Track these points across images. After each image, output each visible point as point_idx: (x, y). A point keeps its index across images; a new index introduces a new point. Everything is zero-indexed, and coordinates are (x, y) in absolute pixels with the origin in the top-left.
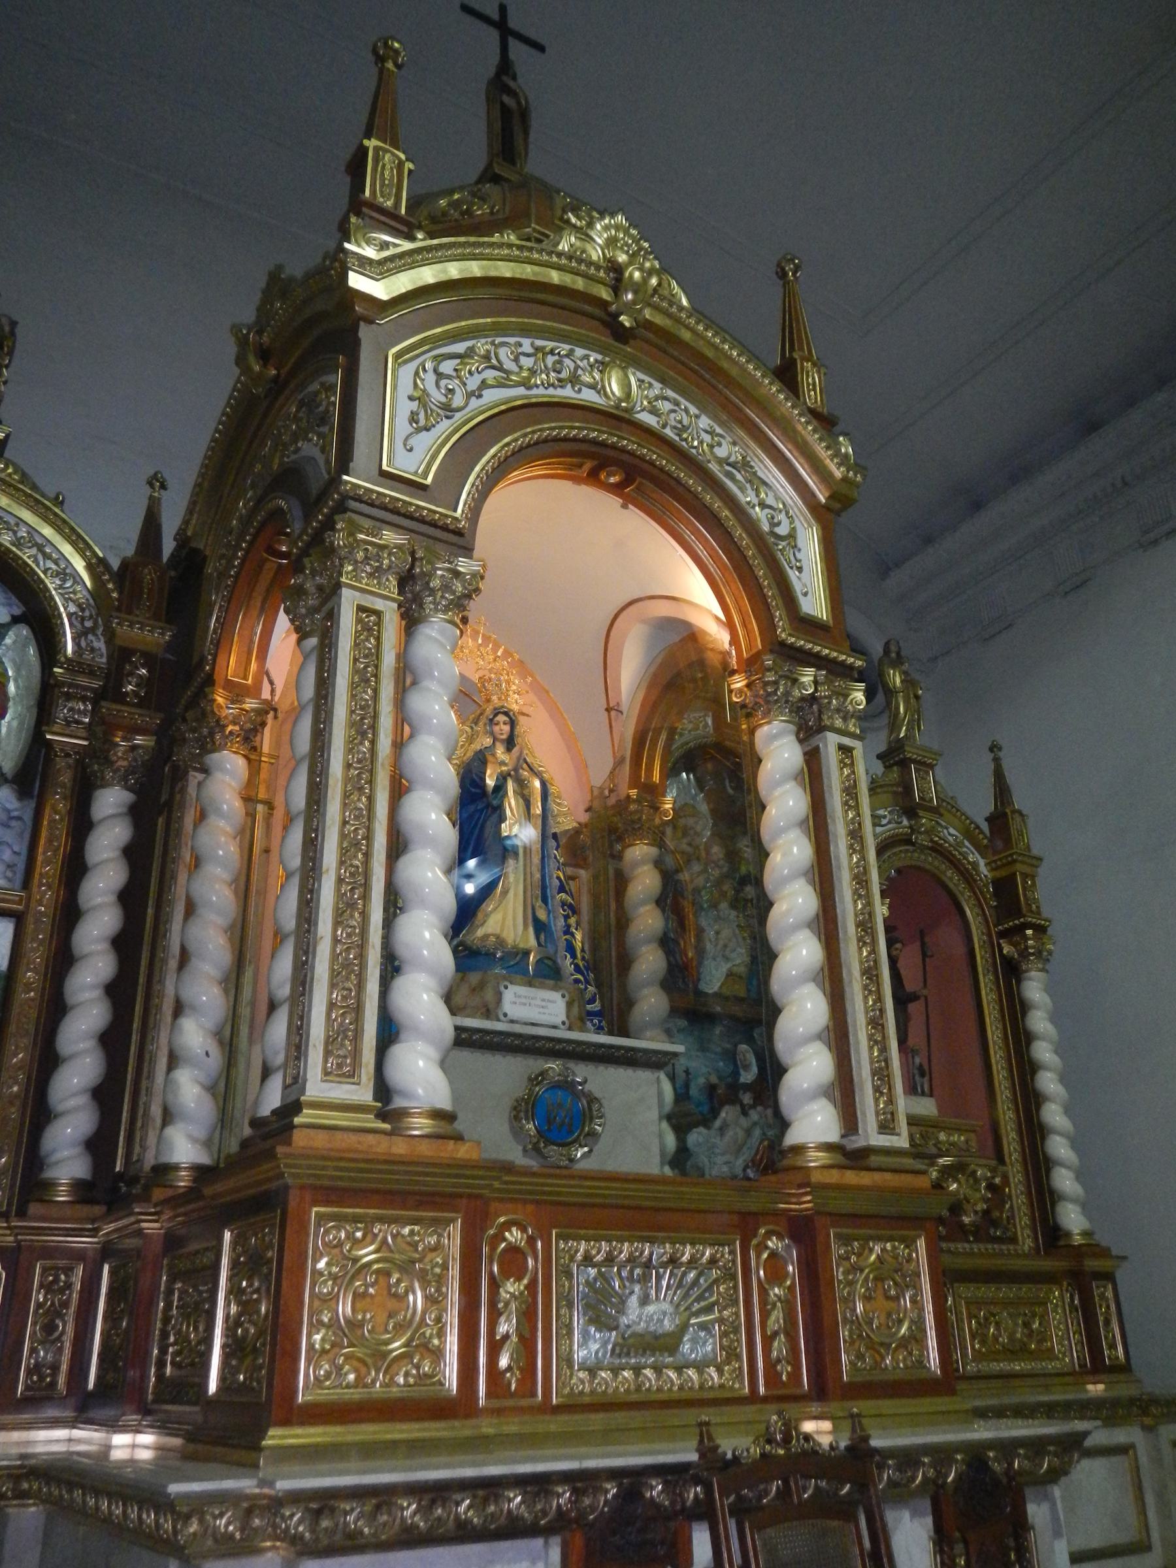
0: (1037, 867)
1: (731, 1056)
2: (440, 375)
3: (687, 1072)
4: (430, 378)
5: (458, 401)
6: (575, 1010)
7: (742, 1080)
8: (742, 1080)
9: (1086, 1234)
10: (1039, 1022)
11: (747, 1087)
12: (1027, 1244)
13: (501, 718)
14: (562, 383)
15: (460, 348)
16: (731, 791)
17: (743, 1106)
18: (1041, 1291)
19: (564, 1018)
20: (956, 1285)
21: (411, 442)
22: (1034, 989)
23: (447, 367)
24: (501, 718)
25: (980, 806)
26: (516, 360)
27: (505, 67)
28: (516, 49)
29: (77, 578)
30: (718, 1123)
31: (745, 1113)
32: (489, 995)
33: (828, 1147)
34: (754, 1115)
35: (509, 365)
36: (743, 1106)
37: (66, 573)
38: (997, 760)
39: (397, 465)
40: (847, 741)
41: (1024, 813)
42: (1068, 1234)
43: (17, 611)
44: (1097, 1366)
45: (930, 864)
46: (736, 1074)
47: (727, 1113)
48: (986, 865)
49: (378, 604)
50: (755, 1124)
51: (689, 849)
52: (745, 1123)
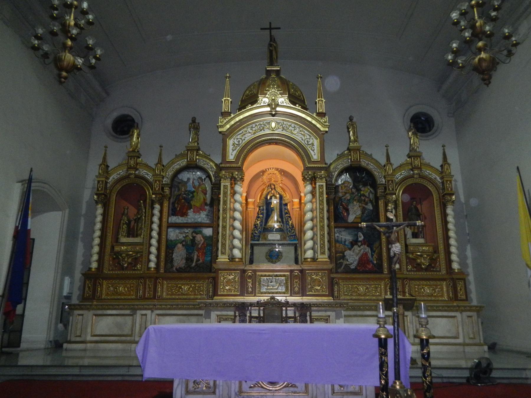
0: (452, 178)
1: (357, 235)
2: (237, 139)
3: (345, 239)
4: (236, 140)
5: (240, 142)
6: (282, 237)
7: (359, 240)
8: (359, 240)
9: (458, 269)
10: (450, 219)
11: (360, 241)
12: (444, 272)
13: (272, 185)
14: (261, 130)
15: (241, 132)
16: (358, 175)
17: (358, 245)
18: (442, 282)
19: (280, 238)
20: (410, 281)
21: (232, 154)
22: (450, 210)
23: (239, 137)
24: (272, 185)
25: (437, 163)
26: (252, 130)
27: (272, 39)
28: (274, 32)
29: (214, 168)
30: (353, 249)
31: (359, 247)
32: (266, 236)
33: (311, 258)
34: (362, 247)
35: (251, 131)
36: (358, 245)
37: (212, 168)
38: (444, 149)
39: (230, 158)
40: (321, 184)
41: (450, 163)
42: (455, 269)
43: (207, 175)
44: (456, 298)
45: (422, 182)
46: (358, 238)
47: (355, 247)
48: (440, 178)
49: (227, 184)
50: (362, 249)
51: (346, 191)
52: (359, 249)
